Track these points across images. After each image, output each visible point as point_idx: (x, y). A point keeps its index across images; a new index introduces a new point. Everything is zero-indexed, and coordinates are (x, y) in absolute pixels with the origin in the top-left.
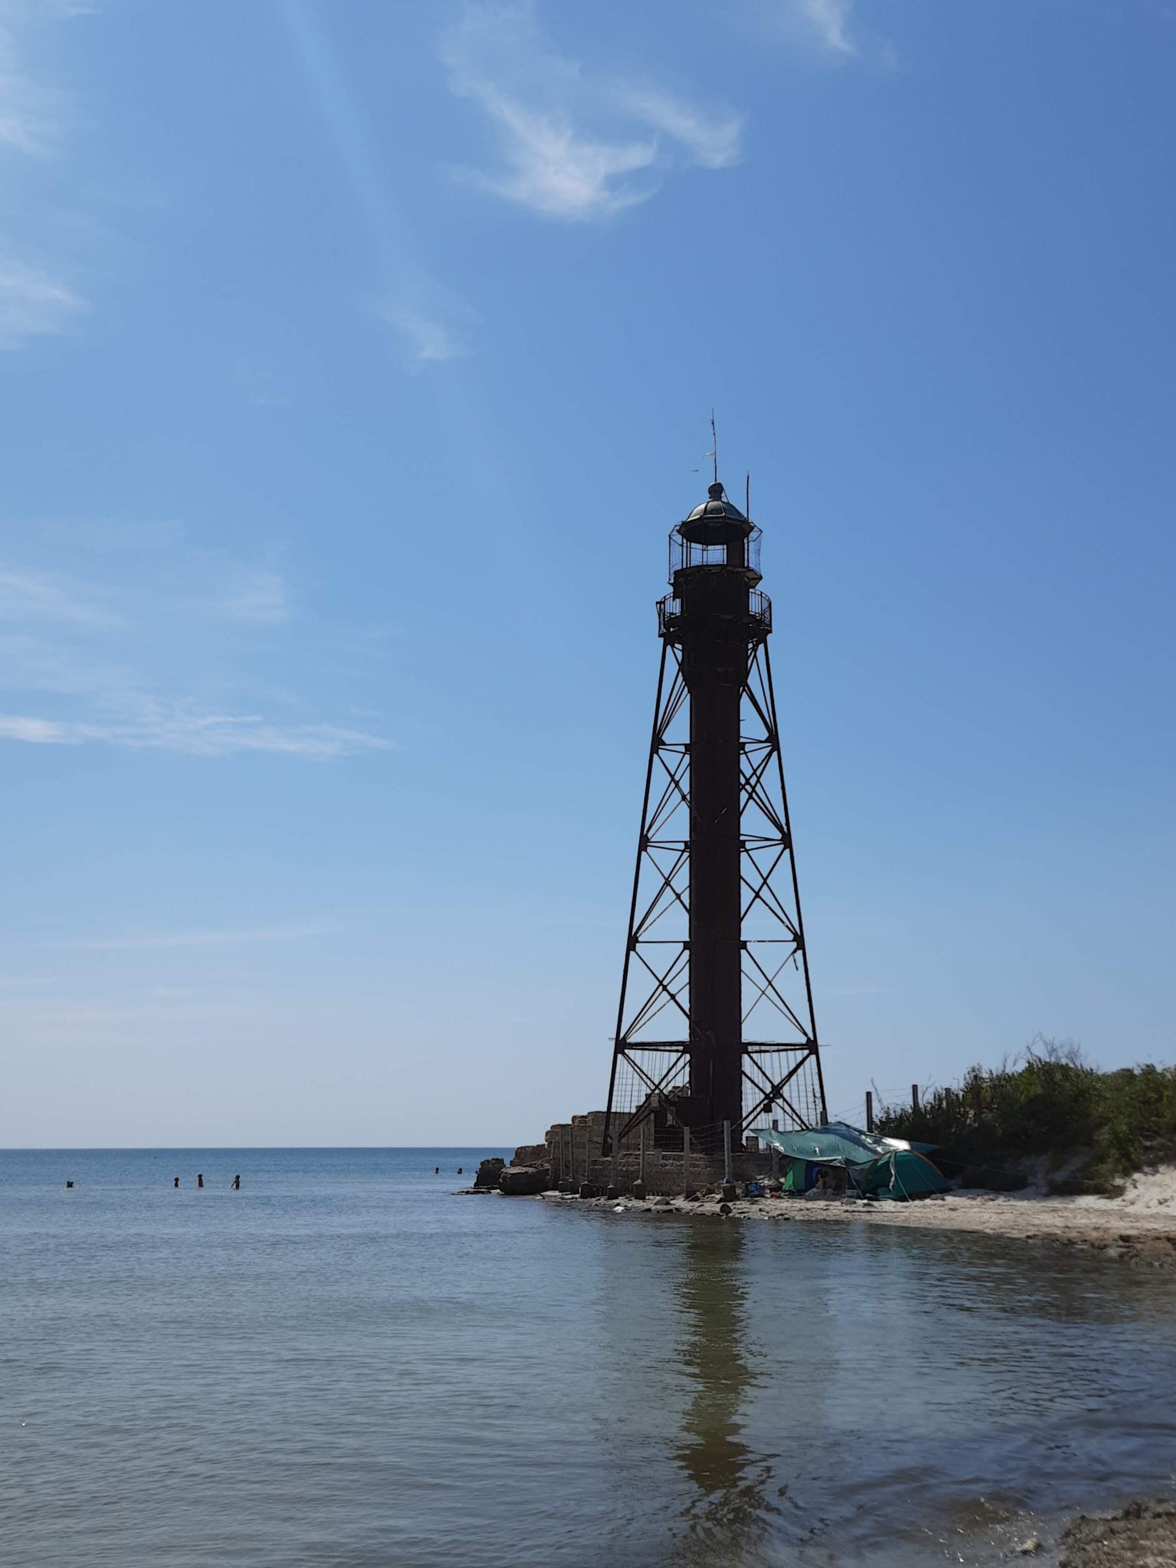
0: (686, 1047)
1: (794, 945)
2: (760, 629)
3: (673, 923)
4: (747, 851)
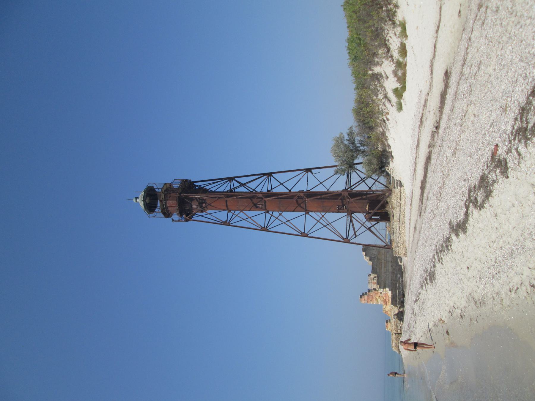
1: (309, 173)
3: (298, 219)
4: (272, 189)
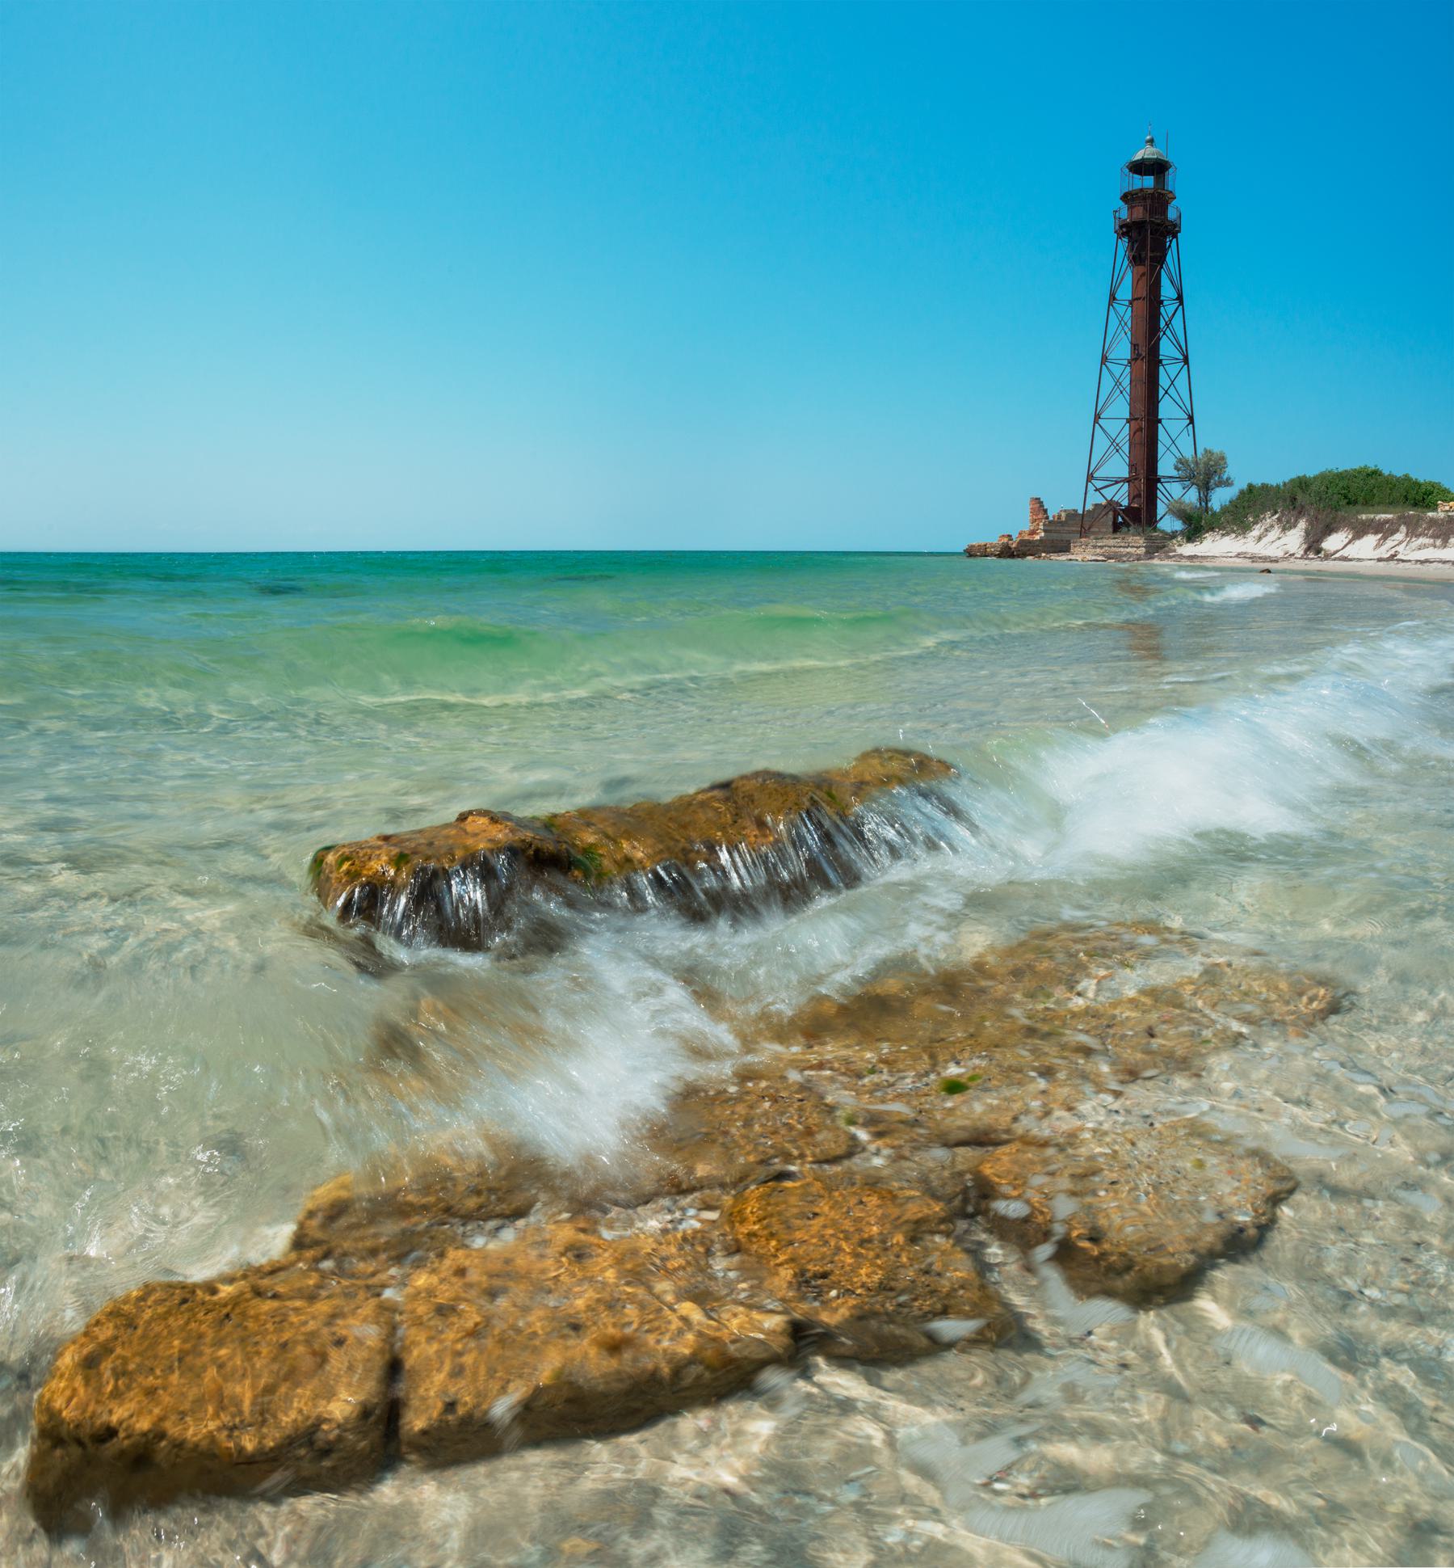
0: (1125, 480)
2: (1173, 230)
3: (1120, 408)
